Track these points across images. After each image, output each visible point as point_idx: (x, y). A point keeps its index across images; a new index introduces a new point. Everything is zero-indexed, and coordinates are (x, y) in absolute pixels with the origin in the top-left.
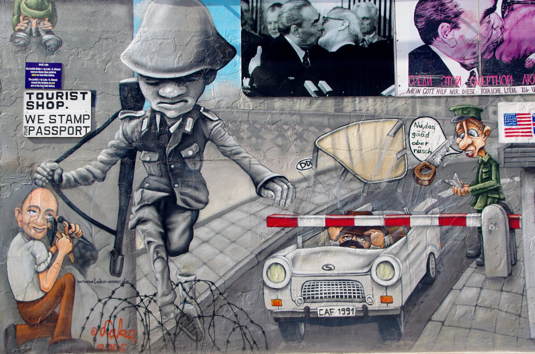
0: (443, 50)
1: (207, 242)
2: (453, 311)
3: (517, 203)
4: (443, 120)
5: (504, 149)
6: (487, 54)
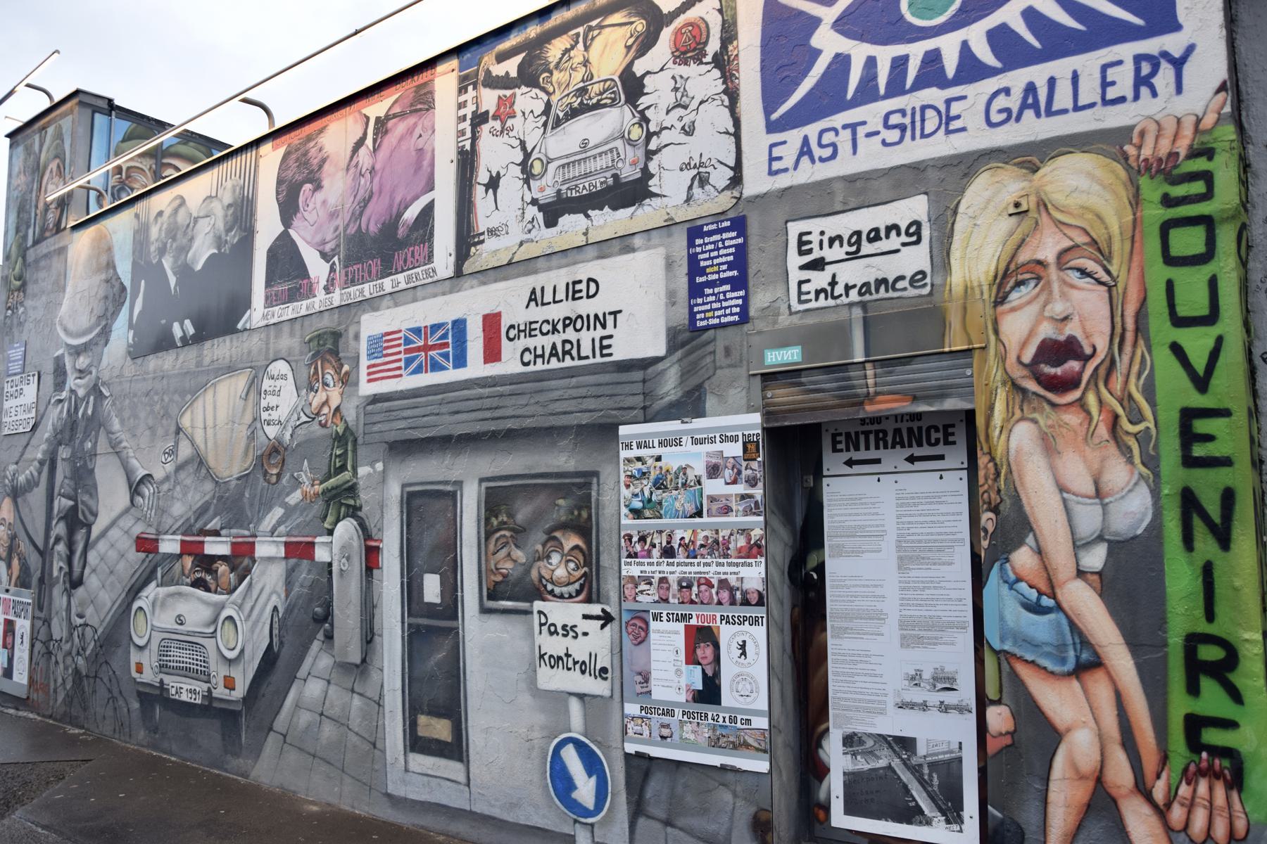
0: (302, 233)
1: (94, 571)
2: (295, 719)
3: (378, 516)
4: (296, 361)
5: (365, 407)
6: (351, 225)
